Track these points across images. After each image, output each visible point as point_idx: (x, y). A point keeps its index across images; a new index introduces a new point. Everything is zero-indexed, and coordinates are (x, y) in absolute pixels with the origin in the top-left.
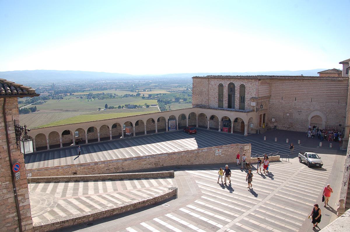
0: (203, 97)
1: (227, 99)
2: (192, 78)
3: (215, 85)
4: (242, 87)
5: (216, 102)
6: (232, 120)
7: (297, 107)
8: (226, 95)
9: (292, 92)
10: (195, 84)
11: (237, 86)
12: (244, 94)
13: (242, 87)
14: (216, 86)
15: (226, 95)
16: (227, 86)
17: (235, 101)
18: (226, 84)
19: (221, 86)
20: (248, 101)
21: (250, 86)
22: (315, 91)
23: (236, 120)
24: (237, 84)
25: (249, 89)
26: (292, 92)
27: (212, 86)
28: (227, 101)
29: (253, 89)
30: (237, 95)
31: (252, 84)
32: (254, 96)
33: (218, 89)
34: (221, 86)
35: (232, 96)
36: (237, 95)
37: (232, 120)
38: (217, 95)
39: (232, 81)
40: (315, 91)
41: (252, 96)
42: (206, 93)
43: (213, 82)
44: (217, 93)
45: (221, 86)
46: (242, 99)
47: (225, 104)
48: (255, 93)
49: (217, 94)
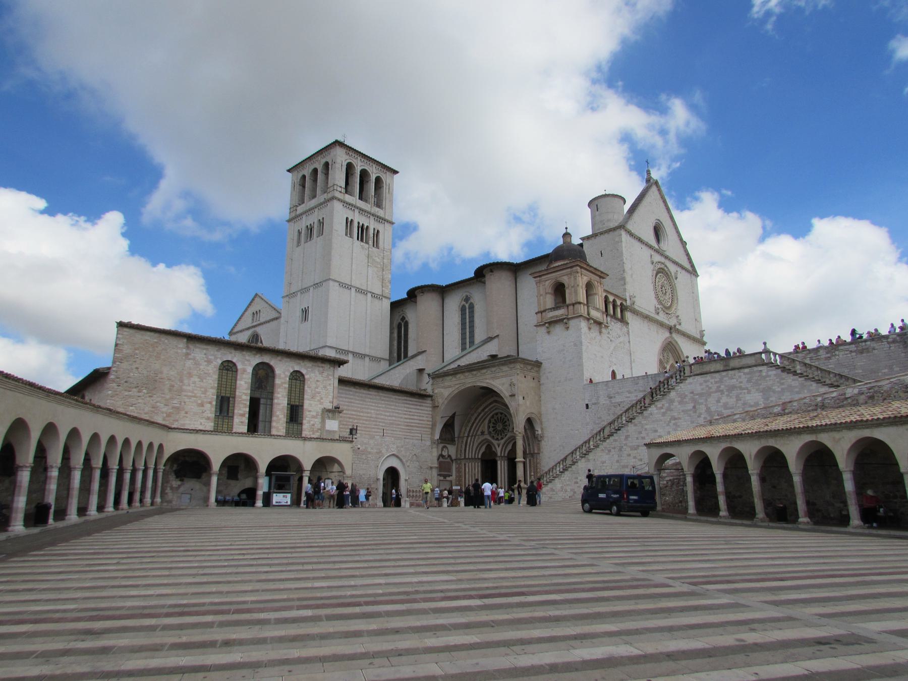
0: (159, 399)
1: (247, 410)
2: (121, 325)
3: (209, 362)
4: (297, 378)
5: (208, 418)
6: (307, 465)
10: (127, 349)
11: (283, 376)
12: (301, 398)
13: (297, 378)
14: (212, 366)
15: (244, 397)
16: (250, 370)
17: (274, 418)
18: (246, 364)
19: (228, 368)
20: (313, 417)
21: (320, 378)
23: (323, 464)
24: (283, 370)
25: (314, 386)
27: (197, 364)
28: (247, 416)
29: (325, 387)
30: (281, 400)
31: (325, 374)
33: (216, 377)
34: (228, 368)
35: (262, 401)
36: (281, 400)
37: (307, 465)
39: (266, 359)
41: (321, 403)
42: (173, 386)
43: (199, 353)
44: (212, 388)
45: (228, 370)
46: (295, 414)
47: (240, 421)
48: (331, 397)
49: (215, 391)
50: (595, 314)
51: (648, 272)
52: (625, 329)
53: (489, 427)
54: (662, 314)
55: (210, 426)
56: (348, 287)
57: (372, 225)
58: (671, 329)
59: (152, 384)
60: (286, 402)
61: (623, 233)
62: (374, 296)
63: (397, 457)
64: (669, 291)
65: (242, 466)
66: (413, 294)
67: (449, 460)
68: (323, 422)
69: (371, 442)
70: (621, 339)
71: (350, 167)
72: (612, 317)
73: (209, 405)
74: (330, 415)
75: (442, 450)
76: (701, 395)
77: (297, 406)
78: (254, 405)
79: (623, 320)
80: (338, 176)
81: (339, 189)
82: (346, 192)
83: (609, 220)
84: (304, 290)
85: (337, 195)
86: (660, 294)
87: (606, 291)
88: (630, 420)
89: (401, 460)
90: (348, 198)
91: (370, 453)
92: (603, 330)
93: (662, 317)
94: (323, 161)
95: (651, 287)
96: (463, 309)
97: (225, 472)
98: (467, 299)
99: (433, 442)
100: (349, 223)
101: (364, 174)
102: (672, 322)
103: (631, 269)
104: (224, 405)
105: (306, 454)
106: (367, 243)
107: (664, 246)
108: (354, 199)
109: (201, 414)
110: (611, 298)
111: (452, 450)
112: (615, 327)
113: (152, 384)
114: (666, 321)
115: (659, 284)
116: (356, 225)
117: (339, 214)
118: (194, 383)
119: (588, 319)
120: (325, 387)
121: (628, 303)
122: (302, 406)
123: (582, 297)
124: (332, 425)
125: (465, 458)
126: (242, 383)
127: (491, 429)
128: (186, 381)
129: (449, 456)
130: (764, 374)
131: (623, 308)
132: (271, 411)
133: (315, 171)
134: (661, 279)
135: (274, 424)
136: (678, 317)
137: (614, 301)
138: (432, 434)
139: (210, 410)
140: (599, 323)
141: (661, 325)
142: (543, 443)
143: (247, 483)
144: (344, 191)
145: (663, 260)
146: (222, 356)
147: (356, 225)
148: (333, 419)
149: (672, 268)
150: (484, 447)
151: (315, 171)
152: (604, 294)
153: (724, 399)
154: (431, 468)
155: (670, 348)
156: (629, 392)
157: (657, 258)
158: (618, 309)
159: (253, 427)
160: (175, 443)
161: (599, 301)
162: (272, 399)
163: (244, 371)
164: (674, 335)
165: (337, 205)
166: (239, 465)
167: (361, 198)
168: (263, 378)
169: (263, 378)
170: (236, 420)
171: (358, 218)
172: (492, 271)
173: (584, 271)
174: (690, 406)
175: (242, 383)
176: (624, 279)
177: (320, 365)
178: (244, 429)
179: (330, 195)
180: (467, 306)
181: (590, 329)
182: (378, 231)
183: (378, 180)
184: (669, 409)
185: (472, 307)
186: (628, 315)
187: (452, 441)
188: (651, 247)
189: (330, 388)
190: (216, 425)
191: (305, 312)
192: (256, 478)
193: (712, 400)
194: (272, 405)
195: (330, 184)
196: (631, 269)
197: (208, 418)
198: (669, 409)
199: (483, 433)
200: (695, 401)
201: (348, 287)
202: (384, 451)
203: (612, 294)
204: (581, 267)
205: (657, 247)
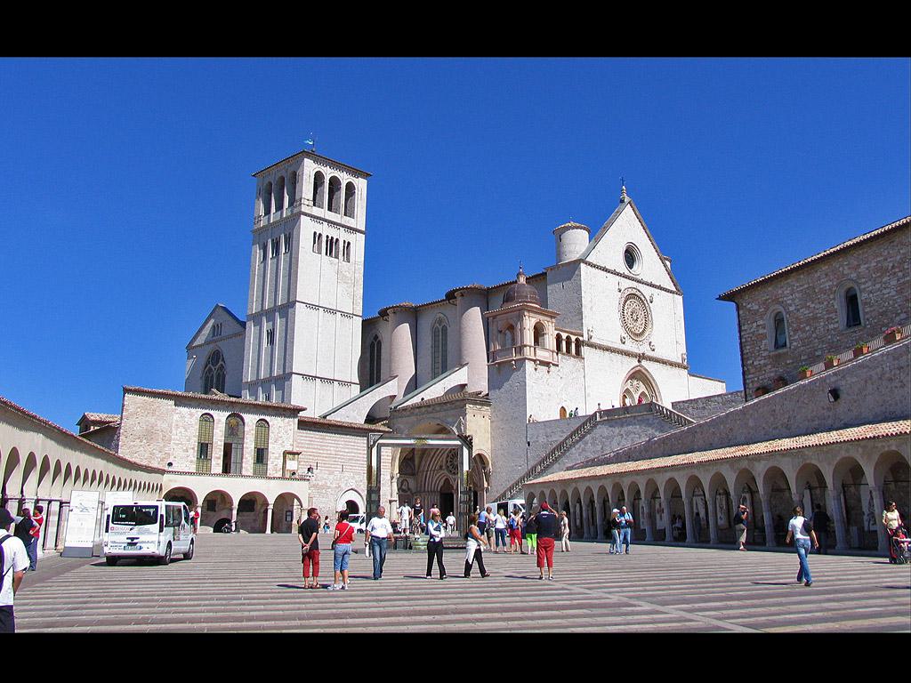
3: (191, 415)
4: (263, 424)
6: (271, 501)
7: (320, 484)
8: (219, 443)
9: (311, 450)
13: (263, 424)
15: (219, 443)
16: (224, 419)
19: (207, 419)
20: (276, 458)
22: (347, 450)
24: (251, 420)
26: (311, 450)
27: (183, 417)
29: (286, 432)
32: (290, 449)
34: (207, 419)
37: (271, 501)
38: (194, 443)
40: (347, 450)
44: (194, 436)
46: (261, 456)
49: (196, 439)
50: (542, 355)
51: (616, 299)
53: (447, 462)
54: (628, 341)
55: (193, 469)
56: (317, 307)
57: (342, 235)
58: (641, 357)
59: (149, 435)
60: (253, 446)
61: (582, 265)
62: (344, 314)
63: (356, 491)
64: (641, 317)
65: (219, 501)
66: (384, 313)
67: (409, 493)
68: (284, 462)
69: (331, 477)
70: (574, 375)
71: (319, 177)
72: (563, 354)
73: (192, 451)
74: (291, 456)
75: (402, 485)
76: (607, 438)
77: (263, 449)
78: (228, 450)
79: (578, 353)
80: (307, 189)
81: (307, 202)
82: (314, 205)
83: (570, 252)
84: (270, 314)
85: (304, 209)
86: (629, 321)
87: (556, 329)
88: (556, 460)
90: (316, 211)
91: (329, 488)
92: (552, 368)
93: (630, 346)
94: (291, 170)
95: (617, 316)
96: (435, 333)
97: (206, 505)
98: (440, 321)
99: (392, 478)
100: (317, 237)
101: (334, 183)
102: (644, 349)
103: (591, 302)
104: (204, 449)
105: (271, 491)
106: (337, 257)
107: (637, 269)
108: (323, 212)
109: (185, 458)
110: (564, 336)
111: (412, 483)
112: (567, 364)
113: (149, 435)
114: (636, 351)
115: (628, 312)
116: (324, 239)
117: (307, 228)
118: (181, 432)
119: (535, 361)
120: (286, 432)
122: (267, 449)
123: (529, 338)
124: (292, 465)
125: (424, 491)
126: (218, 431)
127: (449, 464)
128: (174, 432)
129: (409, 489)
130: (650, 422)
131: (579, 344)
132: (242, 454)
133: (282, 179)
134: (633, 305)
135: (244, 465)
136: (650, 343)
137: (568, 338)
138: (393, 470)
139: (193, 454)
140: (549, 363)
141: (627, 354)
142: (492, 478)
143: (224, 515)
145: (635, 284)
146: (201, 412)
147: (324, 239)
148: (293, 460)
149: (647, 291)
150: (442, 481)
151: (282, 179)
152: (557, 332)
153: (624, 442)
154: (390, 502)
155: (638, 375)
156: (563, 432)
157: (626, 283)
158: (573, 346)
159: (226, 470)
160: (170, 482)
161: (550, 341)
162: (243, 444)
163: (220, 420)
164: (644, 363)
166: (217, 500)
167: (330, 209)
168: (235, 429)
169: (235, 429)
170: (214, 462)
171: (327, 231)
172: (462, 295)
173: (531, 314)
174: (599, 447)
175: (218, 431)
177: (283, 413)
178: (219, 469)
179: (296, 211)
180: (440, 328)
181: (536, 369)
182: (349, 243)
183: (350, 187)
184: (584, 450)
185: (445, 330)
186: (585, 350)
187: (413, 474)
188: (618, 274)
189: (291, 433)
190: (198, 468)
191: (271, 334)
192: (232, 510)
193: (615, 443)
194: (243, 449)
195: (297, 198)
196: (591, 302)
197: (191, 462)
198: (584, 450)
199: (441, 467)
200: (603, 443)
201: (317, 307)
202: (343, 485)
203: (565, 332)
204: (529, 311)
205: (627, 273)
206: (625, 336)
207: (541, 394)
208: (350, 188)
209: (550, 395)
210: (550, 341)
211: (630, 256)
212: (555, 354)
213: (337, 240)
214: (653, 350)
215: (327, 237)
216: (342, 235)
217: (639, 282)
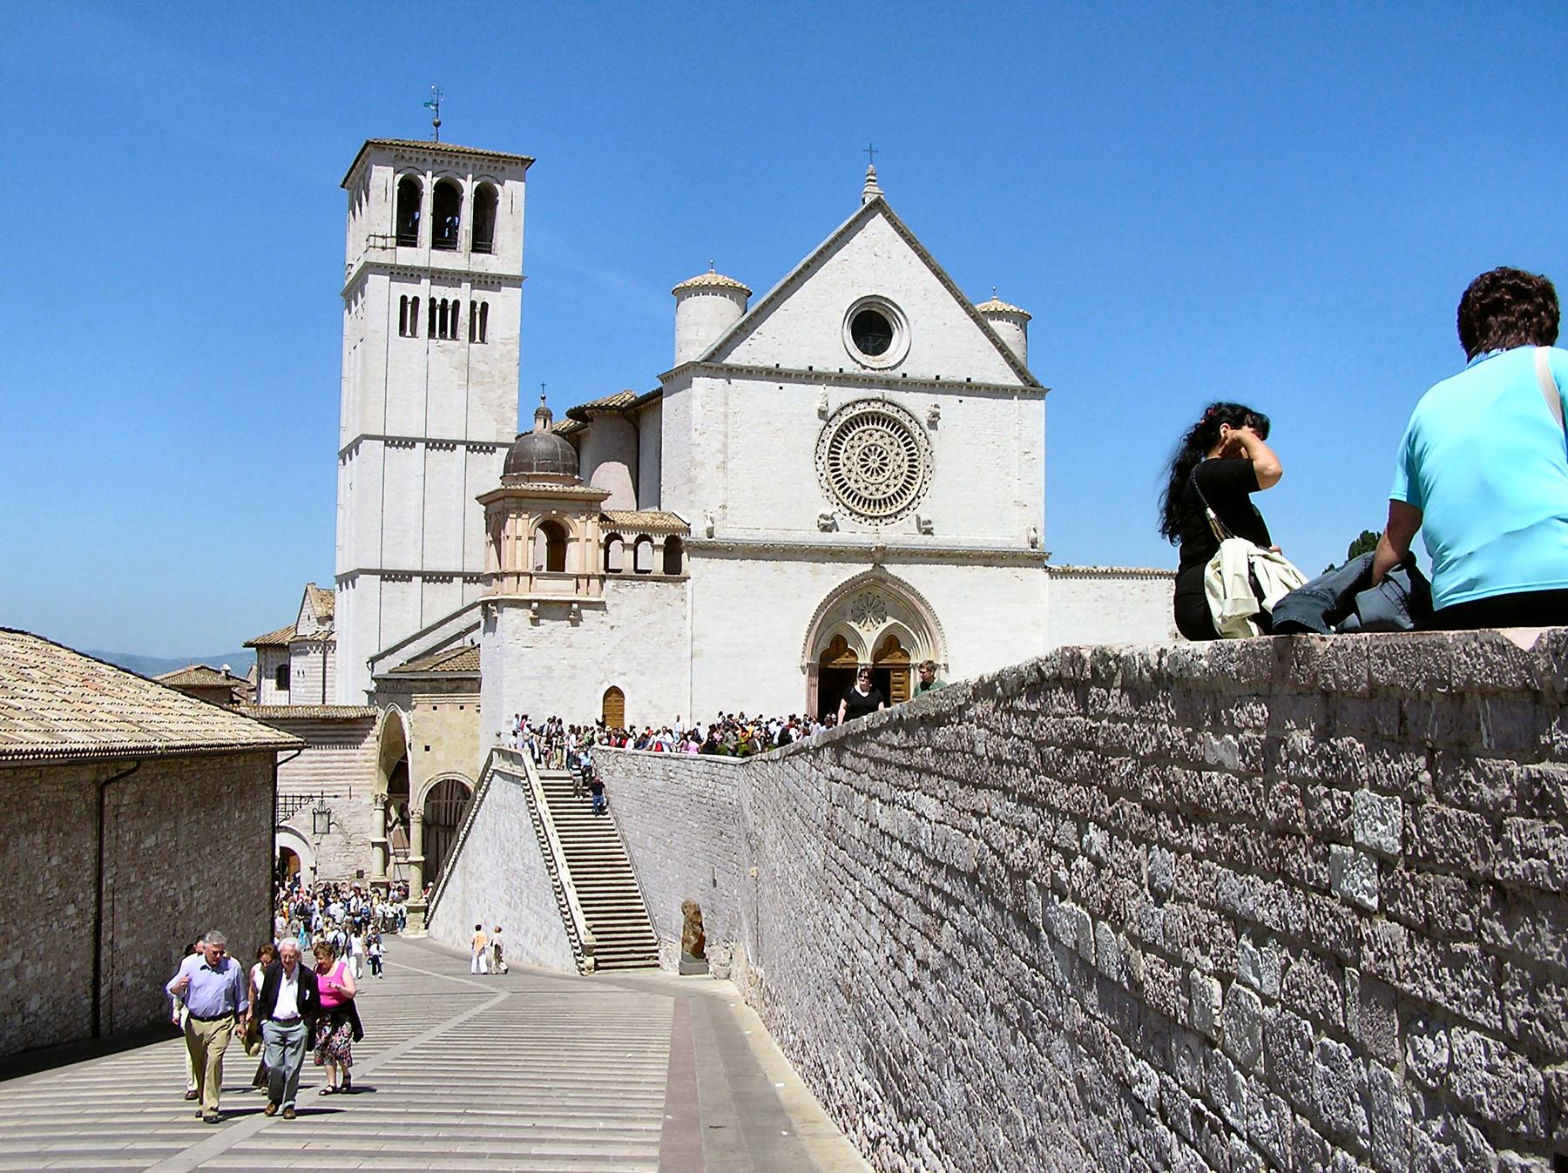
52: (670, 589)
56: (409, 443)
83: (688, 343)
89: (299, 836)
93: (854, 532)
100: (408, 307)
116: (424, 307)
121: (698, 533)
131: (673, 550)
144: (392, 242)
147: (424, 307)
164: (893, 569)
165: (377, 282)
176: (690, 480)
182: (485, 306)
186: (689, 564)
206: (829, 513)
207: (550, 669)
208: (486, 202)
209: (574, 667)
210: (582, 554)
211: (871, 325)
212: (595, 583)
213: (456, 303)
214: (928, 532)
215: (432, 301)
216: (464, 295)
217: (889, 384)
